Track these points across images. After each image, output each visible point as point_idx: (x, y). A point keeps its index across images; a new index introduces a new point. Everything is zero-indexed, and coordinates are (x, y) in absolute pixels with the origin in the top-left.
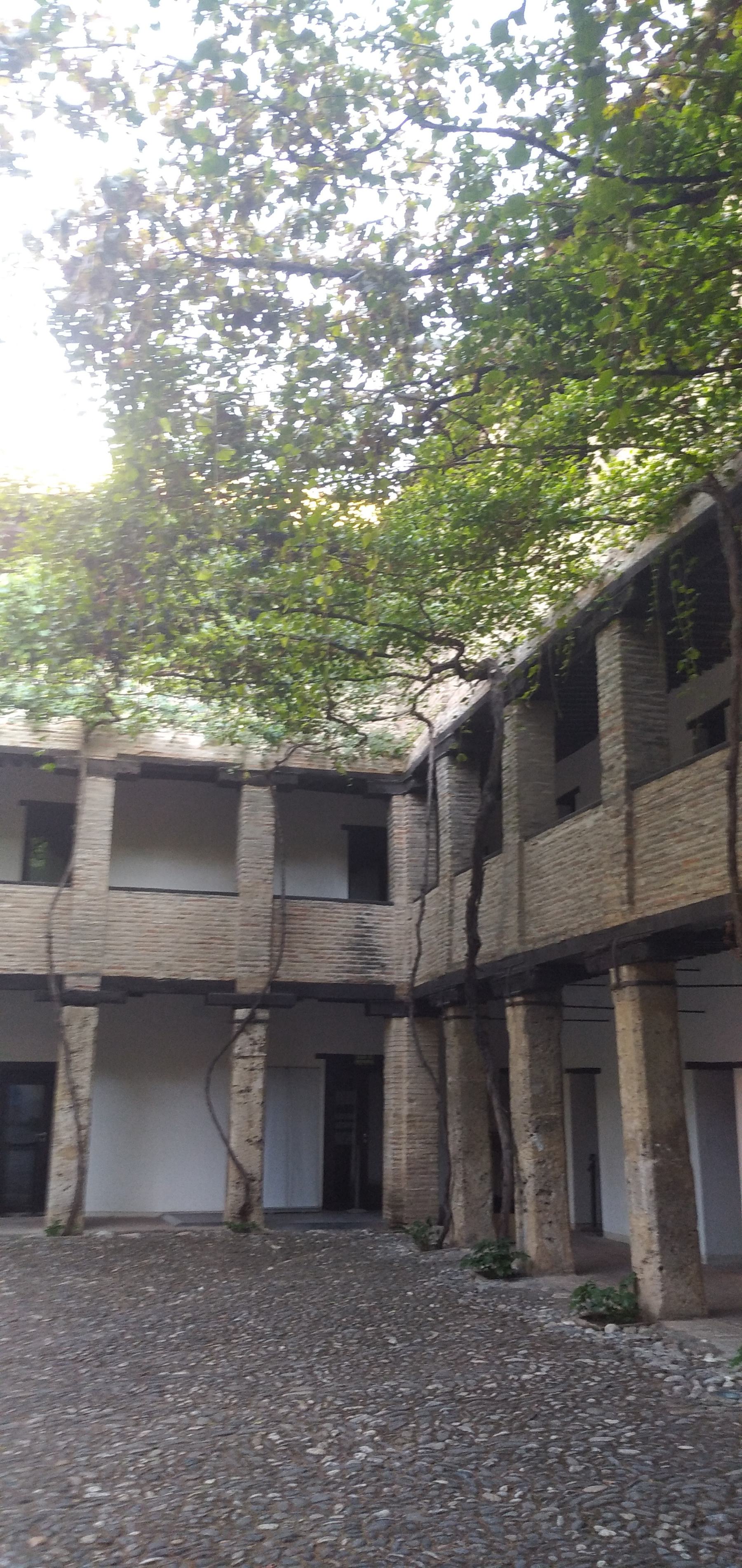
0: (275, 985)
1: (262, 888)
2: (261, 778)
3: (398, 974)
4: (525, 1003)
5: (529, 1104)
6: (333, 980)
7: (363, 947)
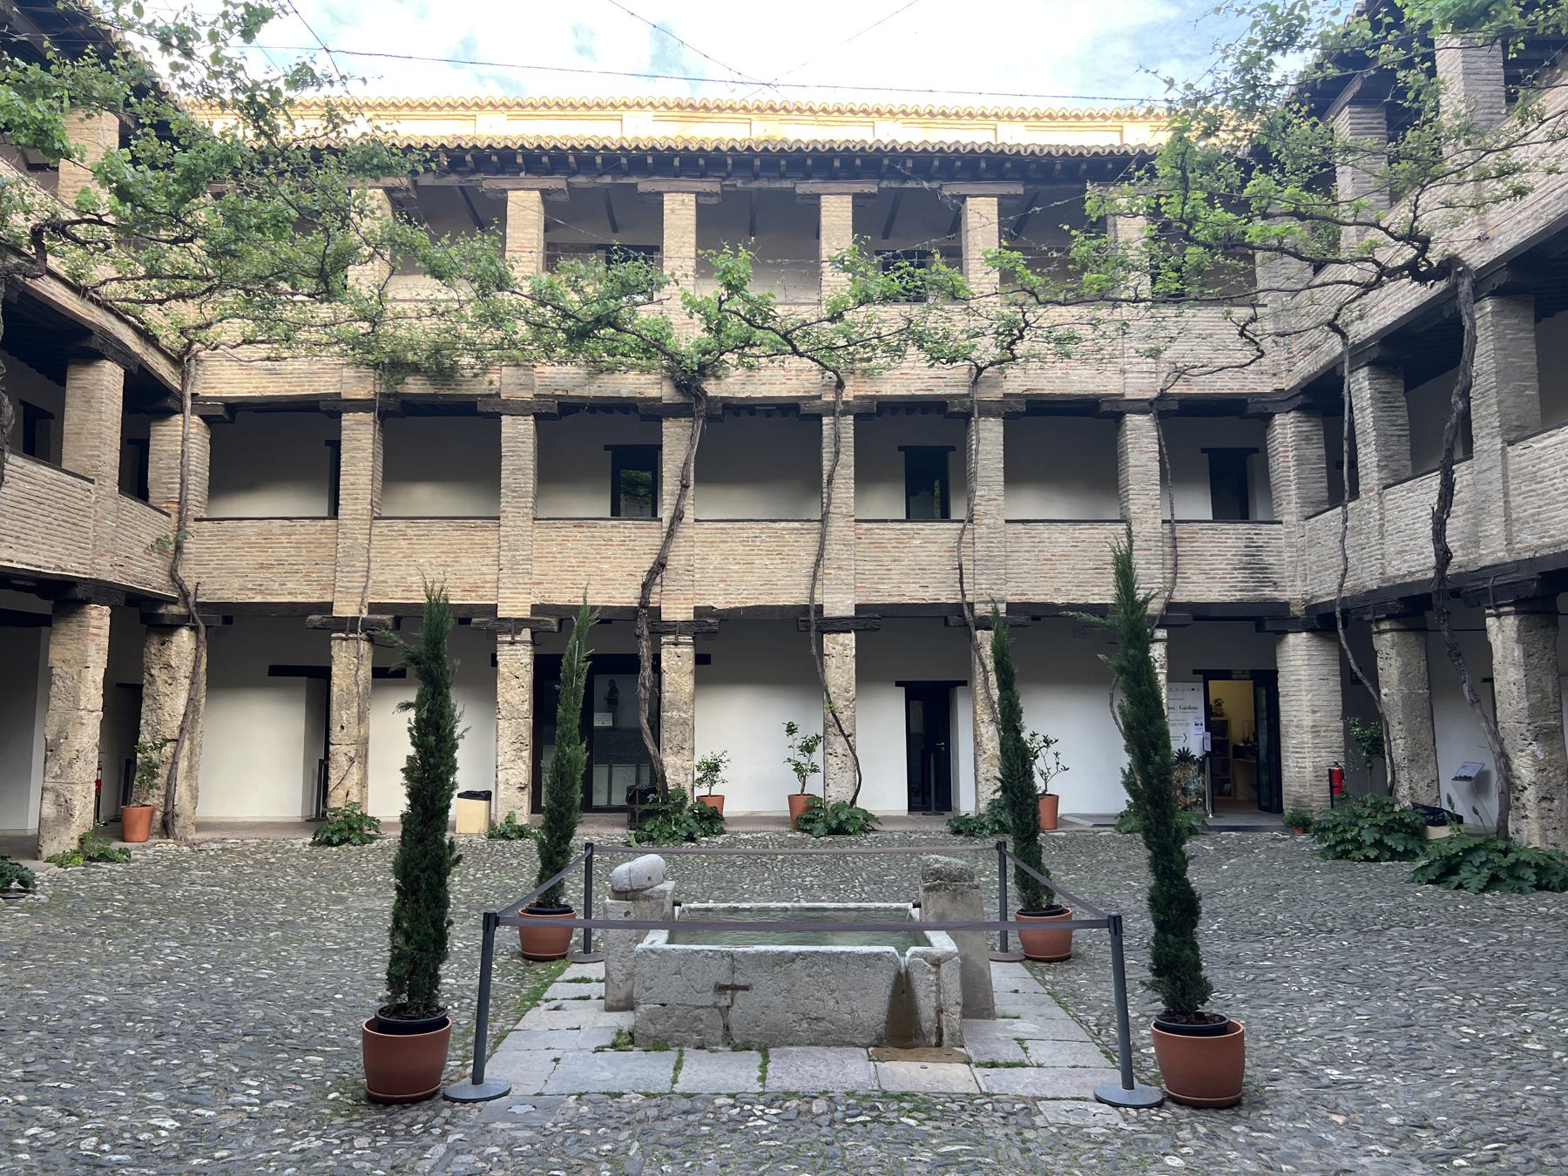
0: (1171, 606)
1: (1151, 513)
2: (1141, 407)
3: (1294, 591)
4: (1517, 613)
5: (1526, 713)
6: (1227, 600)
7: (1255, 567)
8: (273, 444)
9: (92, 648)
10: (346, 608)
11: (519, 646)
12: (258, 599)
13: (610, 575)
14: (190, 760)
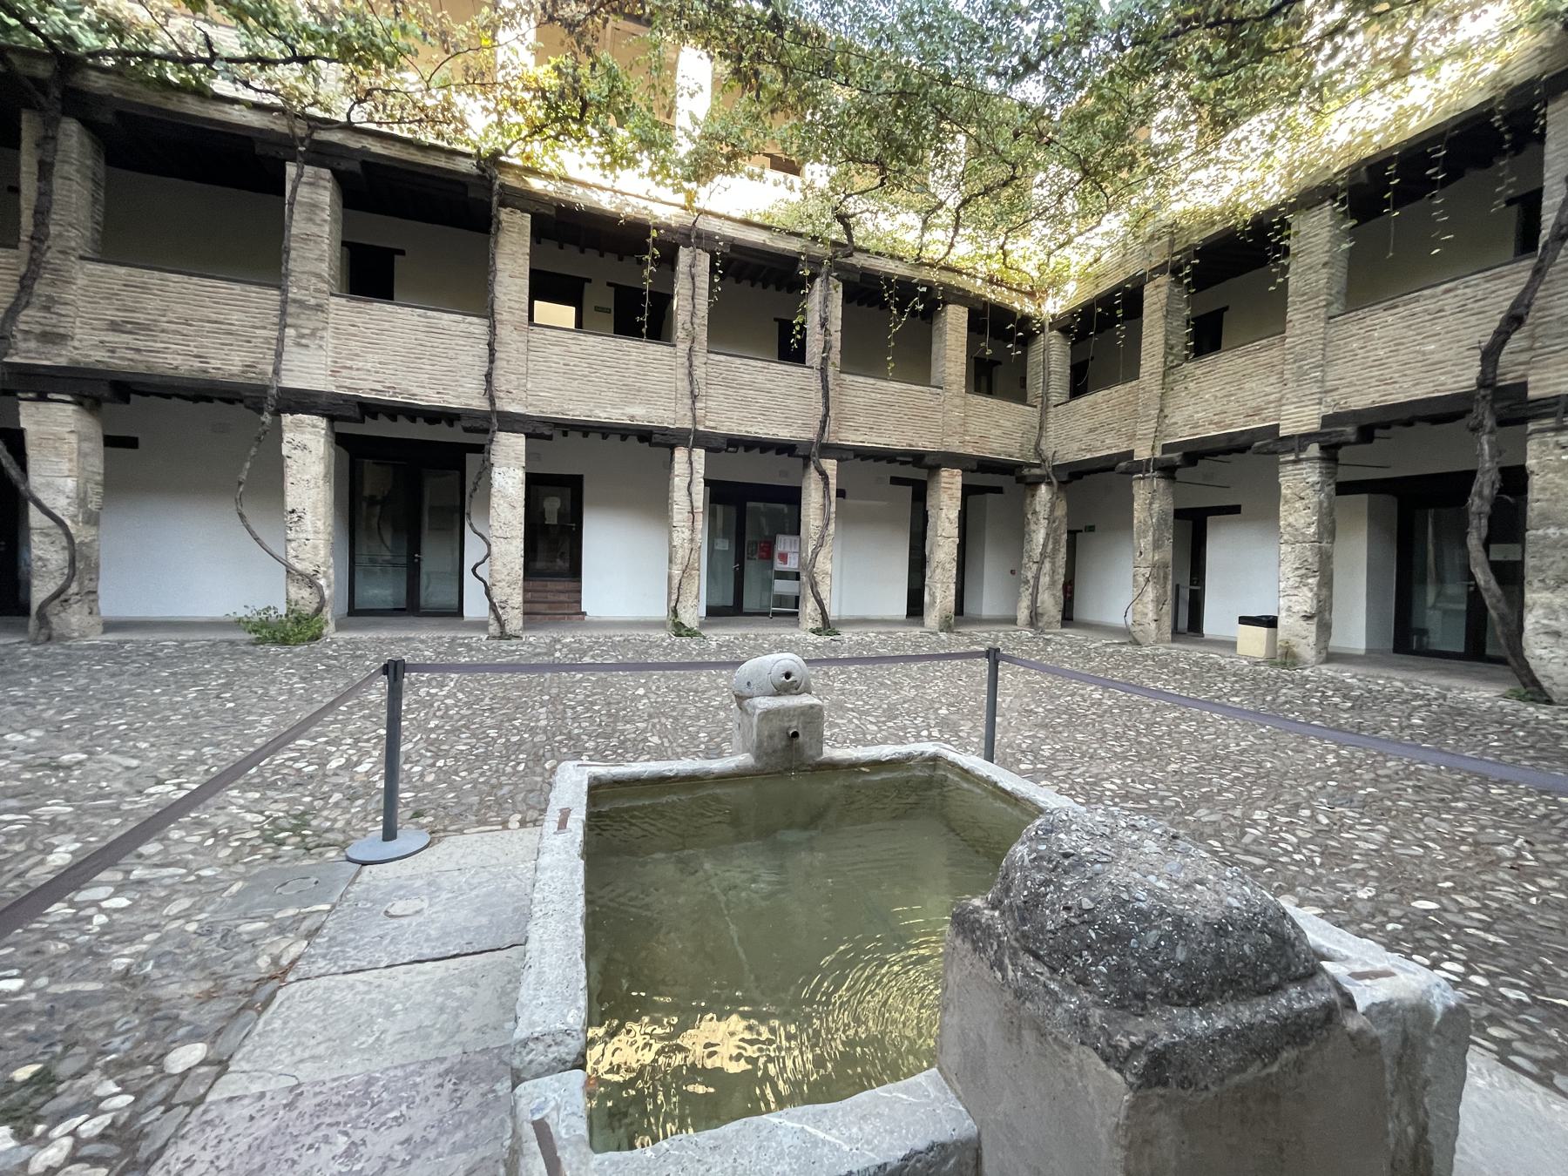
8: (1102, 334)
9: (944, 497)
10: (1142, 453)
11: (1304, 465)
12: (1088, 456)
13: (1436, 357)
14: (1052, 577)
